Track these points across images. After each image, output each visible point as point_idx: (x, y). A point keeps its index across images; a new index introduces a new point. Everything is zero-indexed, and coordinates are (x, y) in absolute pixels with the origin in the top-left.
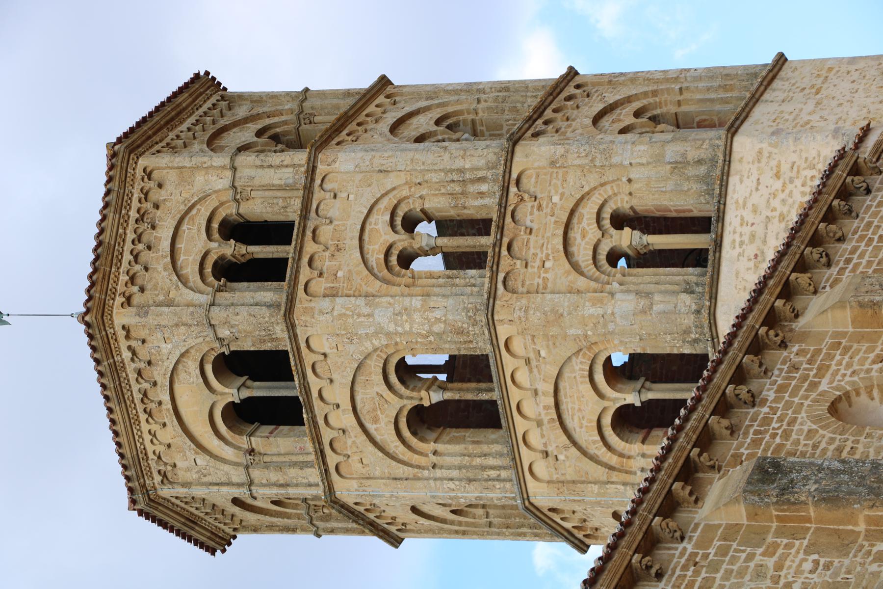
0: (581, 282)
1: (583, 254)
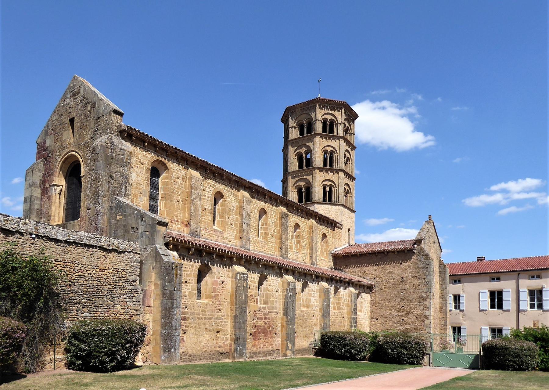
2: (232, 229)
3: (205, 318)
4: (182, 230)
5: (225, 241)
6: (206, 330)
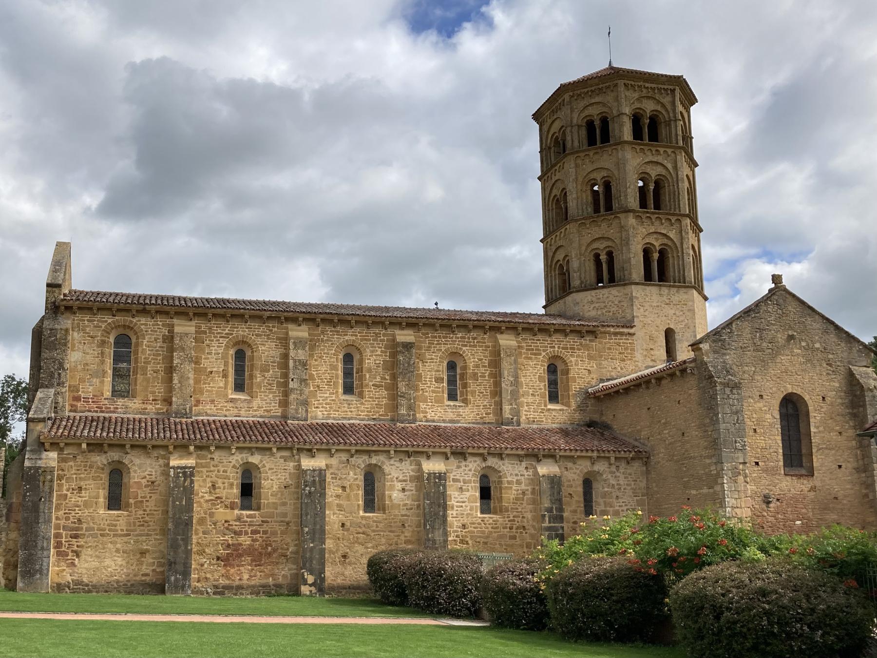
0: (584, 248)
1: (595, 245)
2: (270, 393)
3: (114, 535)
4: (165, 410)
5: (254, 413)
6: (117, 551)
